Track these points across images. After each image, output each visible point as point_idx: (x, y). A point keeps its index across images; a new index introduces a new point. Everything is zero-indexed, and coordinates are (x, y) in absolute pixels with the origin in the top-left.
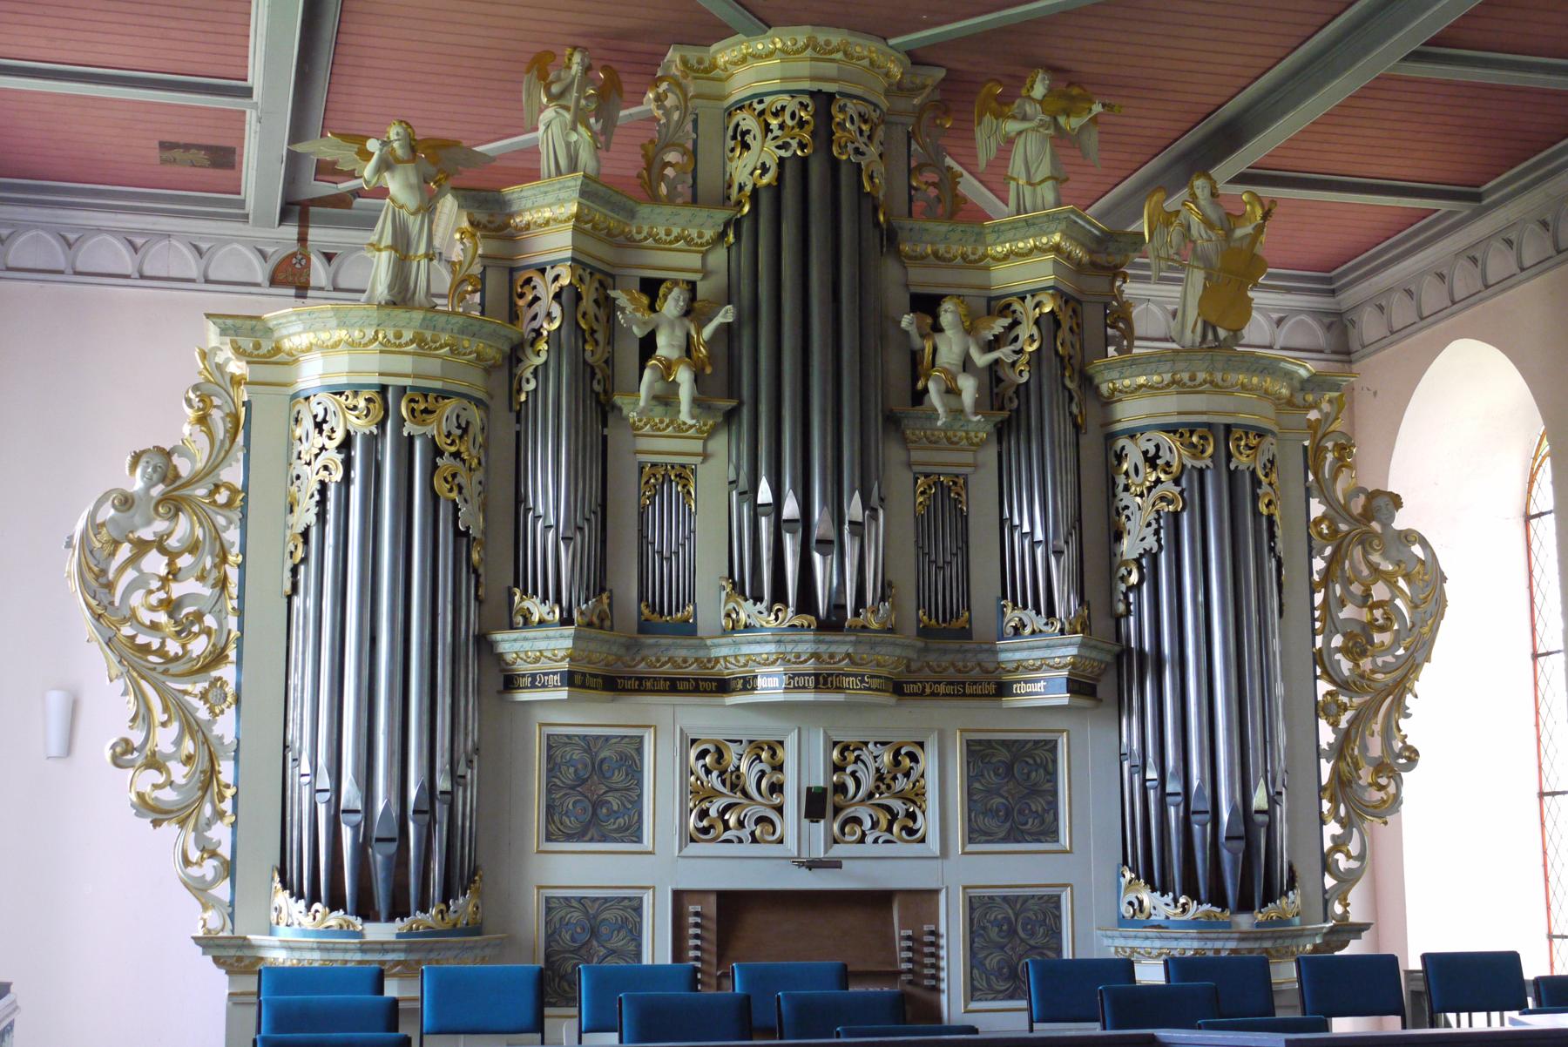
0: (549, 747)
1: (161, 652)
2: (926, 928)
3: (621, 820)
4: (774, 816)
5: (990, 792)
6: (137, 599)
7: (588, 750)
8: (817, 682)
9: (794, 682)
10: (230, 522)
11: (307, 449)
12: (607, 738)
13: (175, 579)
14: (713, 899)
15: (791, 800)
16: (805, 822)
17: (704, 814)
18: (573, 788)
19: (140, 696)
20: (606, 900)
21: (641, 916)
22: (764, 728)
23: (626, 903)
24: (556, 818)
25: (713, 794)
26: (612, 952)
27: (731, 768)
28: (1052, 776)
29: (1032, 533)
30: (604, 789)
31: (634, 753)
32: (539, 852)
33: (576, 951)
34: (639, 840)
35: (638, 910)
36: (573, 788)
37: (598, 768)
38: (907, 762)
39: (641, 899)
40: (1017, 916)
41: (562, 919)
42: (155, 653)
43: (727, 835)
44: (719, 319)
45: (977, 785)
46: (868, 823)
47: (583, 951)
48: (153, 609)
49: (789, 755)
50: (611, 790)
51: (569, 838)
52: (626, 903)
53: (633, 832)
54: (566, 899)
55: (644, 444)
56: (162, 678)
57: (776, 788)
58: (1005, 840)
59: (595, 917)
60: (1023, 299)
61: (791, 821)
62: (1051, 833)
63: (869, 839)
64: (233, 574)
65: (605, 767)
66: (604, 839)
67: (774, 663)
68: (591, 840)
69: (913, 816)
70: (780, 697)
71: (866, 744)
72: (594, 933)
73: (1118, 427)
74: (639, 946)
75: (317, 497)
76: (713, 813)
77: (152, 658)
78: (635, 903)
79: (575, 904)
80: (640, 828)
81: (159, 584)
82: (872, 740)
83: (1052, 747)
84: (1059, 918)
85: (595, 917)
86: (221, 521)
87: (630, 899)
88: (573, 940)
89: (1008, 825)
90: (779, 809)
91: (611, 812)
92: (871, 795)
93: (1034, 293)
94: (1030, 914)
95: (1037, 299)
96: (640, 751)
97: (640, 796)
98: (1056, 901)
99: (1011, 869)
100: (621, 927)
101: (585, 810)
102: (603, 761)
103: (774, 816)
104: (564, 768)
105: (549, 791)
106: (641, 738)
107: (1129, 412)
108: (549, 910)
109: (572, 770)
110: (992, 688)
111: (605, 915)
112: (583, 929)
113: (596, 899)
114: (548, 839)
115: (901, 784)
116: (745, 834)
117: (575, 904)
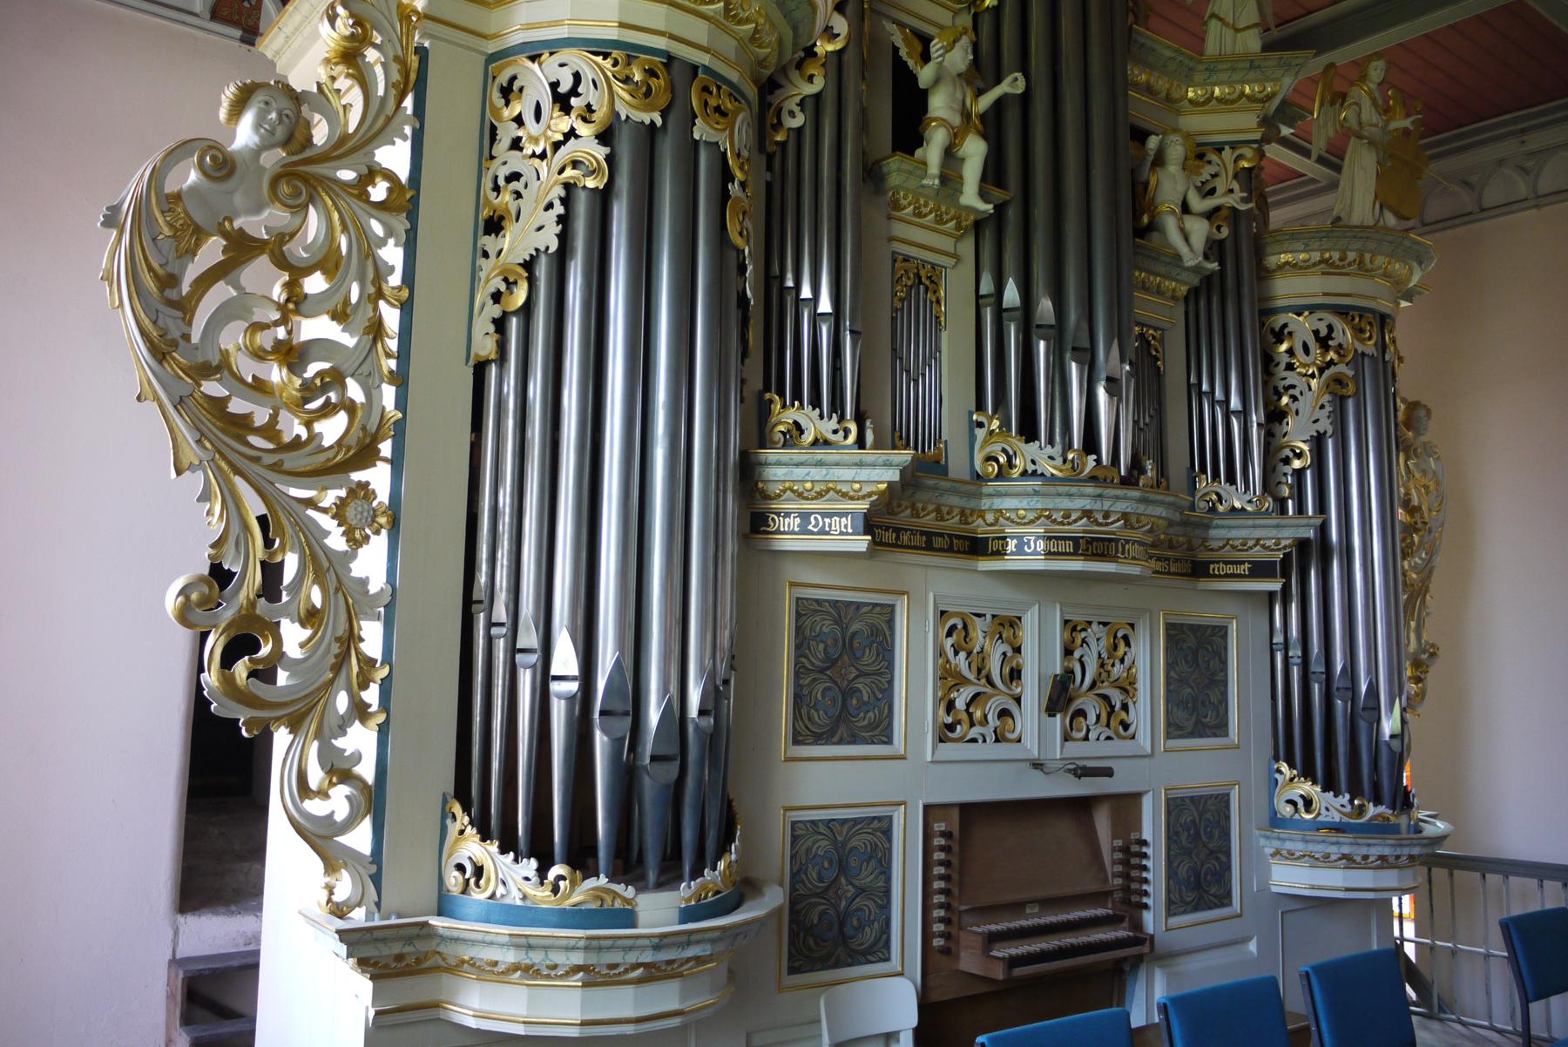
0: (799, 615)
1: (270, 431)
2: (1133, 836)
3: (871, 714)
4: (1013, 707)
5: (1182, 681)
6: (232, 338)
7: (838, 621)
8: (1076, 546)
9: (1058, 545)
10: (390, 232)
11: (536, 135)
12: (859, 605)
13: (297, 312)
14: (955, 813)
15: (1032, 691)
16: (1044, 715)
17: (950, 707)
18: (822, 671)
19: (232, 502)
20: (856, 821)
21: (890, 840)
22: (1003, 599)
23: (876, 824)
24: (804, 711)
25: (962, 681)
26: (861, 891)
27: (977, 649)
28: (1224, 663)
29: (1227, 401)
30: (854, 673)
31: (885, 627)
32: (788, 760)
33: (821, 894)
34: (889, 742)
35: (887, 833)
36: (822, 671)
37: (848, 645)
38: (1122, 648)
39: (890, 818)
40: (1201, 817)
41: (808, 850)
42: (259, 431)
43: (974, 732)
44: (1004, 88)
45: (1172, 674)
46: (1092, 718)
47: (831, 893)
48: (259, 355)
49: (1029, 635)
50: (862, 674)
51: (818, 739)
52: (876, 824)
53: (881, 731)
54: (813, 822)
55: (900, 229)
56: (271, 476)
57: (1015, 675)
58: (1192, 735)
59: (844, 844)
60: (1220, 150)
61: (1029, 717)
62: (1221, 728)
63: (1092, 736)
64: (391, 317)
65: (856, 645)
66: (854, 740)
67: (1032, 522)
68: (840, 742)
69: (1125, 707)
70: (1040, 564)
71: (1090, 623)
72: (843, 867)
73: (1280, 303)
74: (888, 880)
75: (559, 209)
76: (960, 704)
77: (254, 440)
78: (885, 824)
79: (822, 829)
80: (890, 725)
81: (276, 316)
82: (1095, 620)
83: (1222, 632)
84: (1228, 818)
85: (844, 844)
86: (377, 228)
87: (879, 819)
88: (821, 879)
89: (1193, 719)
90: (1018, 700)
91: (862, 704)
92: (1093, 685)
93: (1234, 145)
94: (1209, 816)
95: (1237, 153)
96: (891, 623)
97: (891, 682)
98: (1224, 800)
99: (1197, 767)
100: (870, 858)
101: (834, 700)
102: (854, 634)
103: (1013, 707)
104: (813, 643)
105: (797, 674)
106: (892, 607)
107: (1286, 289)
108: (795, 838)
109: (821, 646)
110: (1187, 568)
111: (854, 842)
112: (831, 862)
113: (844, 821)
114: (796, 742)
115: (1118, 671)
116: (989, 731)
117: (822, 829)
